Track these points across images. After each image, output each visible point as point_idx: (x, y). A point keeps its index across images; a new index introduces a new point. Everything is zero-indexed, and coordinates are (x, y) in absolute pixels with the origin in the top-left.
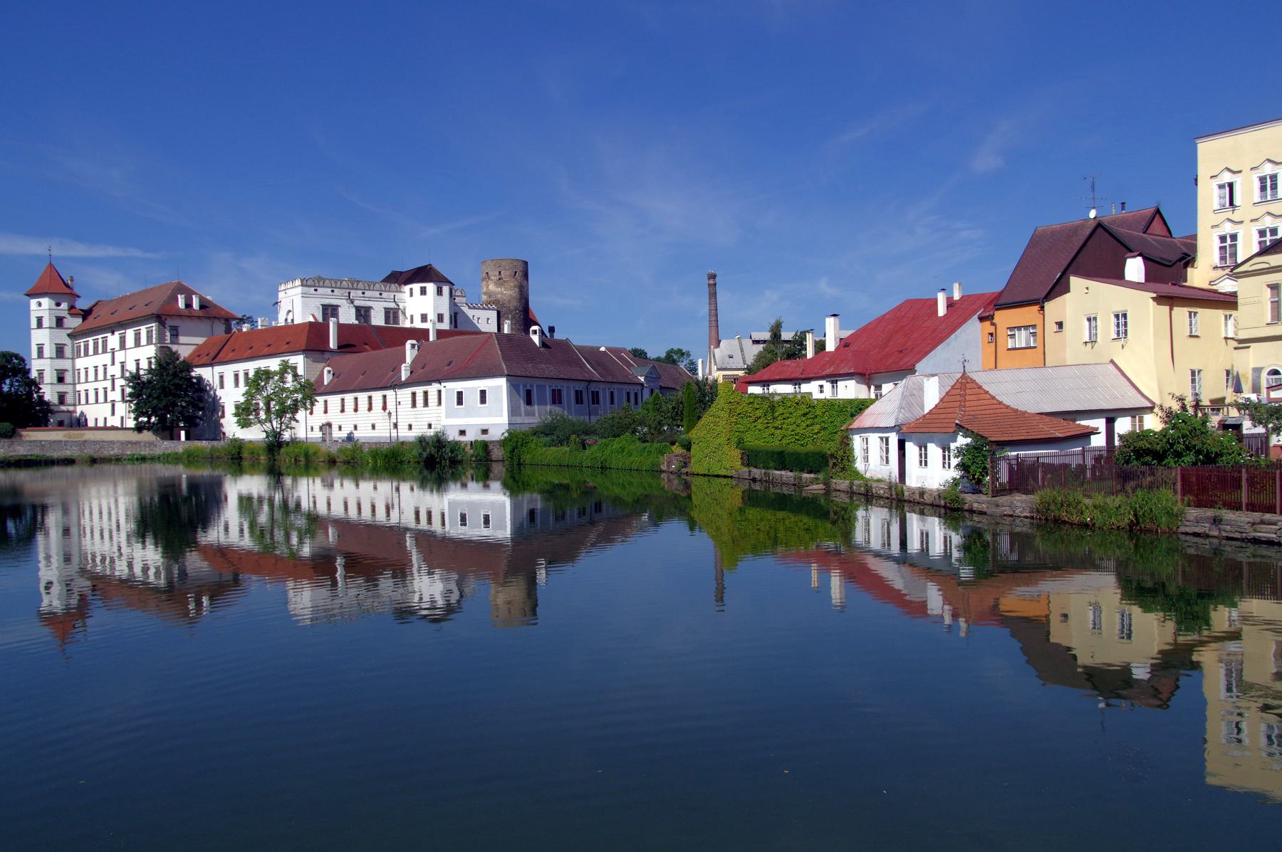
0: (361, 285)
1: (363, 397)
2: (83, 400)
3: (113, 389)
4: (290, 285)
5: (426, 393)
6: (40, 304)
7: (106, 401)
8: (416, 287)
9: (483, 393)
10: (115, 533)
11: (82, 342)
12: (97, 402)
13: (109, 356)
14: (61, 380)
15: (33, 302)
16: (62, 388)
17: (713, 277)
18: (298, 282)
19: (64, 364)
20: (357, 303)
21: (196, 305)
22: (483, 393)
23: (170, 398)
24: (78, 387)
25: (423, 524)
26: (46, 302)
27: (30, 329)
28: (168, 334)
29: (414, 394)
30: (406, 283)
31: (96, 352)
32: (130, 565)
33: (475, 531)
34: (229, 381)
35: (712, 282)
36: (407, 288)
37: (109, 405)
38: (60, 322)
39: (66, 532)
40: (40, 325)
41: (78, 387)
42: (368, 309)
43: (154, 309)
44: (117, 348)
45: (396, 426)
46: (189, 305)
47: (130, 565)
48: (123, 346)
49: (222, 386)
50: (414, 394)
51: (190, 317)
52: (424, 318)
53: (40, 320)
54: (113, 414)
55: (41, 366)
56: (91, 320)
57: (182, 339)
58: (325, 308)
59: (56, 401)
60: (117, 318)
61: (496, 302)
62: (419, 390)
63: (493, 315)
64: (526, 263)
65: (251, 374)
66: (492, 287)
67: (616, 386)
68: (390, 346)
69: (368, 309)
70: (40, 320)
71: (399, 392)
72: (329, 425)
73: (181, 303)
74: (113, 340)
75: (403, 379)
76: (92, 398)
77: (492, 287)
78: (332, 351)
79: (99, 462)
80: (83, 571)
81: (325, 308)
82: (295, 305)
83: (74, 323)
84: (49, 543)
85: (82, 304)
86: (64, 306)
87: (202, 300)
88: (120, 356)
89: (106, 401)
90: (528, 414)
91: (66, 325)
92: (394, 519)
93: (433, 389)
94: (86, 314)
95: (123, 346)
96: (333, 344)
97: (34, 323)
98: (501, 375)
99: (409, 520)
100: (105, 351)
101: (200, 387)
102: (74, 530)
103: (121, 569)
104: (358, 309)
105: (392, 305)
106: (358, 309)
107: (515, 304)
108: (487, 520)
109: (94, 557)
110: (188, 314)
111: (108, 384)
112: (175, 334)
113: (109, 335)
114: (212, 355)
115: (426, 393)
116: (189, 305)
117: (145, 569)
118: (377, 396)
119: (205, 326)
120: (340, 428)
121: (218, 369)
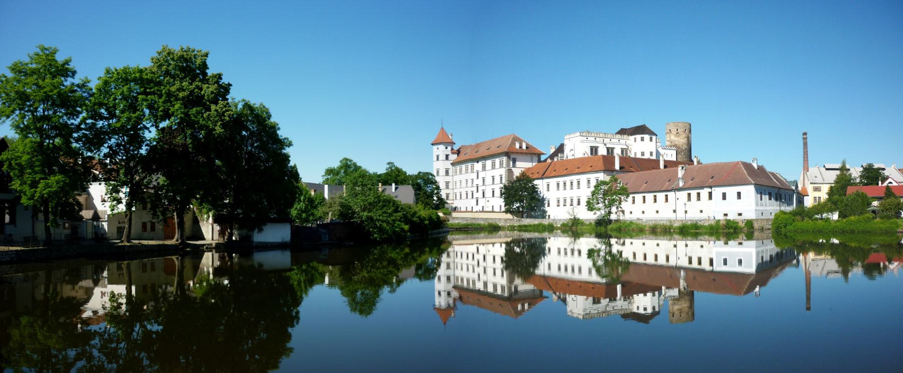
1: (649, 197)
2: (458, 197)
4: (572, 135)
5: (699, 194)
8: (638, 137)
11: (458, 167)
14: (447, 187)
15: (435, 147)
16: (447, 191)
18: (578, 134)
19: (448, 179)
21: (524, 147)
22: (739, 194)
23: (522, 196)
25: (695, 265)
26: (442, 147)
27: (432, 162)
29: (689, 195)
30: (631, 135)
32: (485, 284)
36: (633, 137)
38: (447, 156)
39: (448, 267)
40: (438, 159)
42: (613, 149)
43: (505, 149)
45: (675, 211)
46: (521, 147)
47: (485, 284)
50: (689, 195)
51: (522, 153)
52: (643, 154)
55: (441, 180)
56: (464, 157)
57: (518, 164)
58: (592, 148)
60: (480, 154)
61: (675, 146)
62: (694, 193)
65: (593, 183)
66: (673, 137)
69: (613, 149)
72: (623, 212)
73: (517, 146)
74: (478, 166)
76: (464, 196)
77: (673, 137)
79: (470, 230)
81: (592, 148)
82: (577, 147)
83: (453, 157)
84: (442, 271)
85: (456, 148)
86: (449, 148)
87: (527, 144)
88: (481, 175)
90: (762, 205)
92: (672, 262)
93: (704, 192)
96: (617, 167)
98: (751, 184)
99: (684, 263)
100: (472, 172)
102: (452, 266)
103: (480, 286)
104: (608, 149)
105: (625, 147)
107: (685, 147)
109: (462, 280)
110: (521, 153)
111: (475, 189)
112: (514, 161)
113: (476, 164)
115: (699, 194)
116: (521, 147)
117: (495, 286)
118: (661, 196)
119: (529, 157)
121: (546, 181)
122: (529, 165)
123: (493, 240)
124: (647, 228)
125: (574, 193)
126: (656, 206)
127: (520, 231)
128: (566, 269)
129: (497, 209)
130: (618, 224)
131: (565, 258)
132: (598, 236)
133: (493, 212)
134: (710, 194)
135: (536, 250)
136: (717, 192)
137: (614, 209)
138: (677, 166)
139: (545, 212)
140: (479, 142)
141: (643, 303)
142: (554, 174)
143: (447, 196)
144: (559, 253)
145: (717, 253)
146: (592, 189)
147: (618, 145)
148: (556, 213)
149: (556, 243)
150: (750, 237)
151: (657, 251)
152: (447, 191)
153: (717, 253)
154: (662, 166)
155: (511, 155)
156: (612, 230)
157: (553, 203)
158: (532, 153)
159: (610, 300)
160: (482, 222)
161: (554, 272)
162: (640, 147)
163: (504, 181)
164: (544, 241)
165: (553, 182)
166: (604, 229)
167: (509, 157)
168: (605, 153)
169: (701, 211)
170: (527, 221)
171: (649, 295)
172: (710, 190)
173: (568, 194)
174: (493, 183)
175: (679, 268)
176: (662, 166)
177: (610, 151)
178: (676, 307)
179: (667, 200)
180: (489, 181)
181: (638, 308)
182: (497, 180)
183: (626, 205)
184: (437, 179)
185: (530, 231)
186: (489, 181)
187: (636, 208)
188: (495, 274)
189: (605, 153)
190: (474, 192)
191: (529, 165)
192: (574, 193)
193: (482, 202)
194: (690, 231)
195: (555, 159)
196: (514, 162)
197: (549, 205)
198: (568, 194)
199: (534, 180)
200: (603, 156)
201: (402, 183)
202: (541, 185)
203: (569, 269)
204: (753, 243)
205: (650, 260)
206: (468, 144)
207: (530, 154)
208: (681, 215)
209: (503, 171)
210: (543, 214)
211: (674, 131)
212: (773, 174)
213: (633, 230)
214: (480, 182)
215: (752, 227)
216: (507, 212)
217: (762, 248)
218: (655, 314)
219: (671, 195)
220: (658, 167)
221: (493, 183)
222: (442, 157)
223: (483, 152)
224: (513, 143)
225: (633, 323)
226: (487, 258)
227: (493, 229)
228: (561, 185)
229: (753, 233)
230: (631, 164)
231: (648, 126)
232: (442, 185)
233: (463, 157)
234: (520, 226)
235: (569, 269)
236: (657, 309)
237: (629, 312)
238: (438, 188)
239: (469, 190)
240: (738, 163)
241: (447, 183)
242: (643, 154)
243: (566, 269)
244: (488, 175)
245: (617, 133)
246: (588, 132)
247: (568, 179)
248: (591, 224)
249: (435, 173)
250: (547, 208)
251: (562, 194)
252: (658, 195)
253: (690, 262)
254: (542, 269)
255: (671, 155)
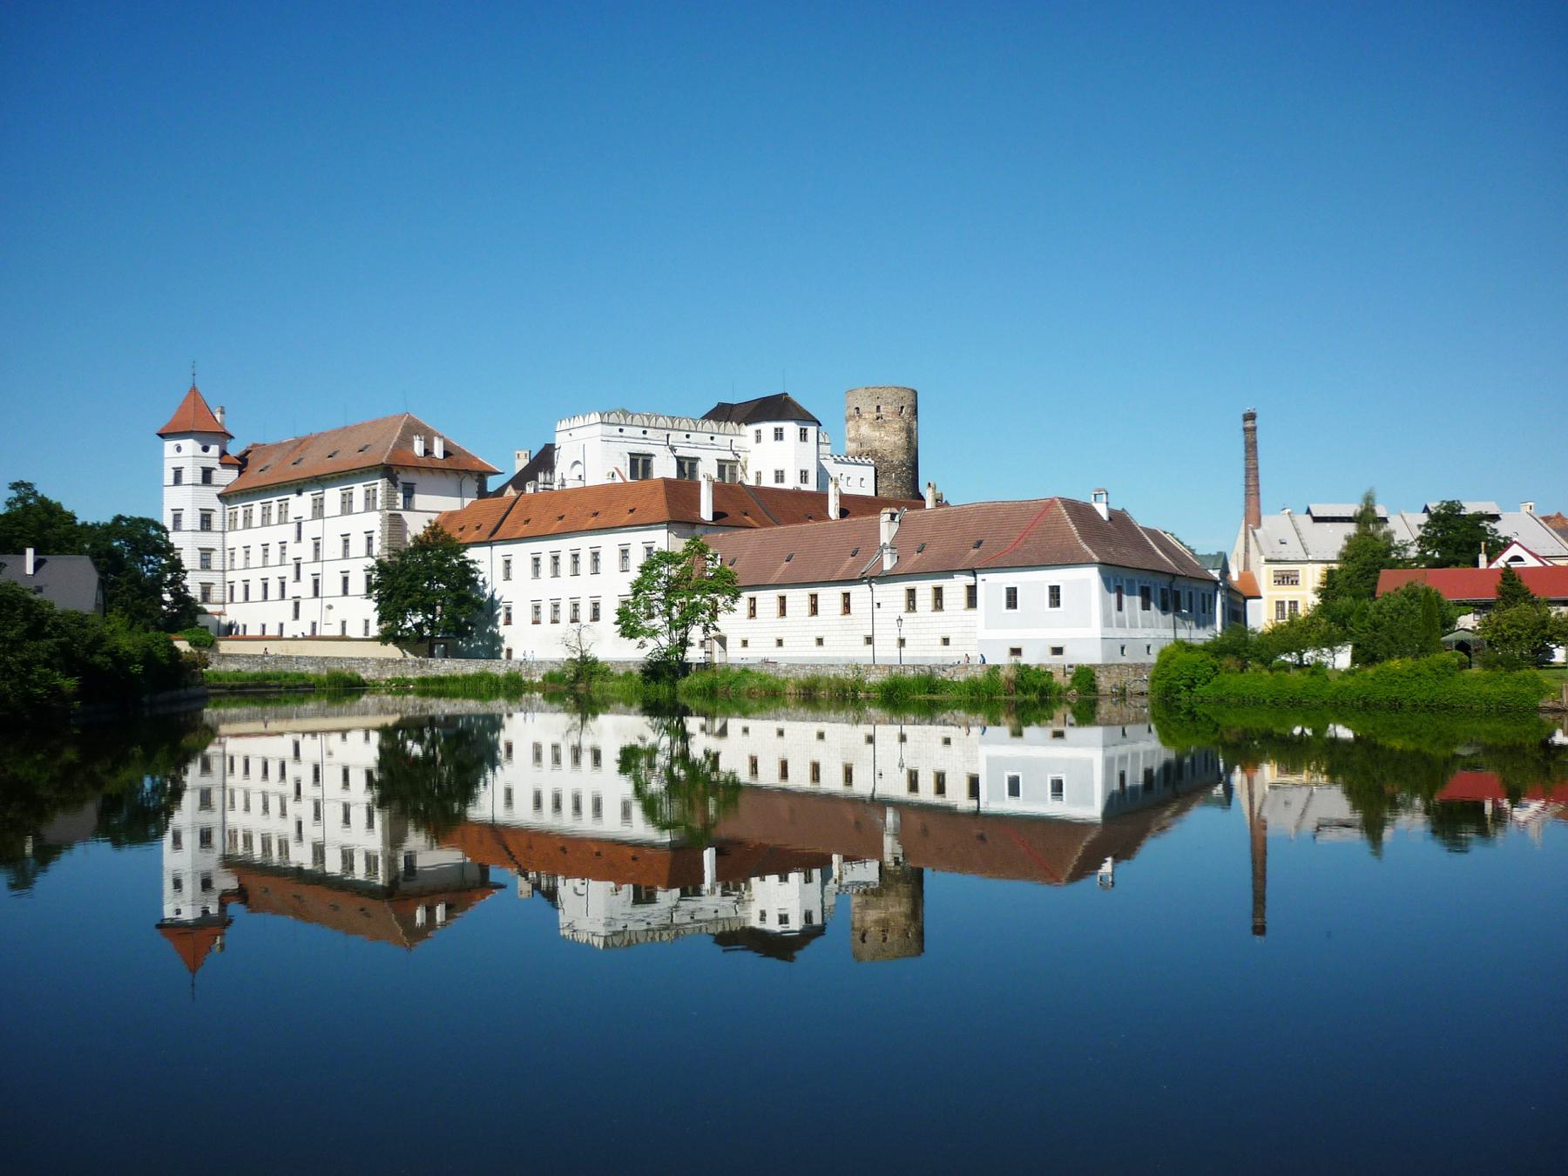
0: (684, 424)
1: (798, 598)
2: (239, 594)
3: (298, 578)
4: (579, 422)
5: (938, 592)
6: (179, 449)
7: (283, 596)
8: (768, 428)
9: (1055, 592)
10: (290, 803)
12: (265, 597)
13: (294, 527)
14: (206, 564)
15: (170, 445)
16: (206, 577)
17: (1250, 417)
18: (595, 418)
19: (208, 540)
20: (678, 453)
21: (438, 451)
22: (1055, 592)
23: (429, 592)
24: (230, 576)
25: (926, 794)
26: (190, 446)
28: (400, 496)
29: (911, 593)
31: (266, 522)
32: (319, 852)
33: (1035, 803)
34: (522, 565)
35: (1249, 424)
37: (290, 605)
38: (207, 475)
39: (205, 801)
40: (177, 480)
41: (230, 576)
42: (694, 461)
44: (307, 512)
45: (869, 640)
46: (428, 452)
47: (319, 852)
48: (318, 510)
49: (507, 577)
50: (911, 593)
51: (431, 470)
52: (779, 476)
53: (178, 473)
54: (296, 616)
55: (186, 544)
57: (420, 500)
58: (634, 458)
59: (199, 599)
60: (307, 469)
61: (872, 453)
62: (924, 588)
63: (869, 473)
64: (915, 393)
66: (865, 430)
67: (1195, 584)
68: (791, 522)
69: (694, 461)
70: (178, 473)
71: (881, 590)
72: (722, 641)
73: (418, 448)
74: (300, 504)
75: (888, 564)
76: (256, 592)
77: (865, 430)
78: (704, 524)
79: (277, 691)
80: (229, 862)
81: (634, 458)
83: (226, 477)
84: (186, 816)
85: (235, 449)
86: (214, 450)
87: (446, 443)
88: (310, 529)
89: (283, 596)
90: (1121, 624)
91: (214, 482)
93: (955, 587)
94: (242, 463)
95: (318, 510)
96: (706, 513)
97: (169, 477)
98: (1090, 563)
99: (895, 787)
100: (283, 521)
101: (466, 576)
102: (216, 797)
103: (301, 856)
104: (680, 461)
105: (729, 456)
106: (678, 458)
108: (1057, 787)
109: (248, 839)
110: (427, 467)
111: (289, 572)
112: (409, 492)
113: (293, 497)
114: (488, 526)
115: (938, 592)
116: (428, 452)
117: (347, 857)
118: (830, 597)
119: (451, 482)
120: (745, 643)
121: (500, 550)
122: (451, 504)
123: (343, 722)
124: (790, 688)
125: (584, 587)
126: (817, 626)
127: (423, 694)
128: (557, 805)
129: (355, 630)
130: (708, 676)
131: (554, 774)
132: (652, 709)
133: (343, 638)
134: (972, 590)
135: (472, 750)
136: (993, 585)
137: (696, 633)
138: (877, 512)
139: (497, 640)
140: (302, 432)
141: (778, 901)
142: (523, 530)
143: (206, 589)
144: (538, 757)
145: (989, 760)
146: (635, 574)
147: (710, 449)
148: (530, 642)
149: (528, 729)
150: (1086, 714)
151: (819, 752)
152: (206, 577)
153: (989, 760)
154: (833, 512)
155: (400, 475)
156: (690, 693)
157: (522, 614)
158: (460, 470)
159: (684, 893)
160: (311, 670)
161: (523, 814)
162: (772, 457)
163: (377, 549)
164: (495, 724)
165: (521, 553)
166: (667, 689)
167: (393, 480)
168: (673, 475)
169: (946, 641)
170: (444, 667)
171: (795, 877)
172: (970, 580)
173: (566, 588)
174: (346, 555)
175: (880, 804)
176: (833, 512)
177: (687, 466)
178: (872, 915)
179: (847, 608)
180: (332, 547)
181: (763, 915)
182: (358, 546)
183: (732, 622)
184: (174, 538)
185: (455, 695)
186: (332, 547)
187: (761, 631)
188: (346, 819)
189: (673, 475)
190: (288, 578)
191: (451, 504)
192: (584, 587)
193: (310, 610)
194: (912, 696)
195: (529, 489)
196: (408, 496)
197: (508, 622)
198: (566, 588)
199: (467, 546)
200: (667, 481)
201: (60, 549)
202: (485, 561)
203: (567, 805)
204: (1095, 733)
205: (799, 779)
206: (271, 440)
207: (457, 472)
208: (886, 651)
209: (374, 521)
210: (493, 646)
211: (869, 414)
212: (1154, 534)
213: (750, 694)
214: (305, 550)
215: (1093, 688)
216: (384, 638)
217: (1121, 750)
218: (812, 932)
219: (859, 593)
220: (822, 514)
221: (346, 555)
222: (191, 474)
223: (314, 463)
224: (405, 440)
225: (748, 959)
226: (325, 773)
227: (343, 688)
228: (546, 563)
229: (1093, 704)
230: (743, 505)
231: (796, 396)
232: (189, 559)
233: (254, 478)
234: (423, 681)
235: (567, 805)
236: (817, 921)
237: (735, 926)
238: (176, 566)
239: (273, 577)
240: (1052, 502)
241: (206, 554)
242: (779, 476)
243: (557, 805)
244: (331, 529)
245: (708, 417)
246: (625, 413)
247: (565, 546)
248: (629, 674)
249: (168, 522)
250: (503, 630)
251: (548, 588)
252: (821, 592)
253: (913, 786)
254: (487, 805)
255: (859, 481)
